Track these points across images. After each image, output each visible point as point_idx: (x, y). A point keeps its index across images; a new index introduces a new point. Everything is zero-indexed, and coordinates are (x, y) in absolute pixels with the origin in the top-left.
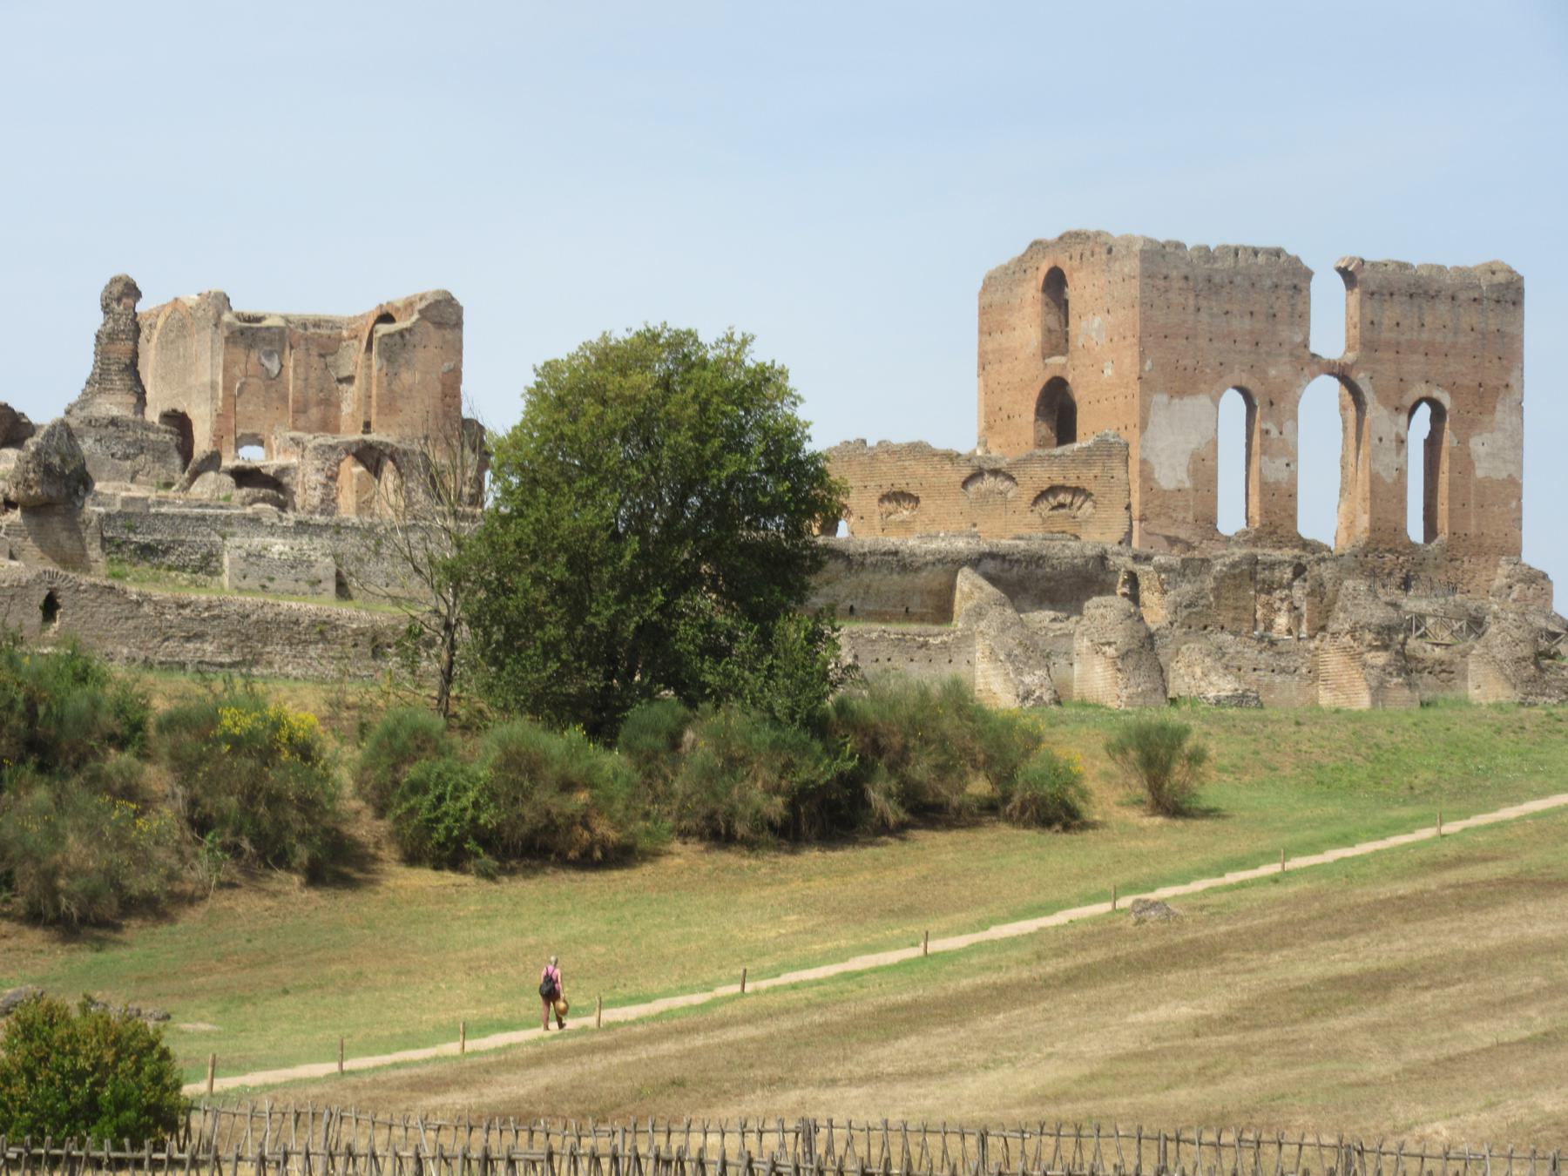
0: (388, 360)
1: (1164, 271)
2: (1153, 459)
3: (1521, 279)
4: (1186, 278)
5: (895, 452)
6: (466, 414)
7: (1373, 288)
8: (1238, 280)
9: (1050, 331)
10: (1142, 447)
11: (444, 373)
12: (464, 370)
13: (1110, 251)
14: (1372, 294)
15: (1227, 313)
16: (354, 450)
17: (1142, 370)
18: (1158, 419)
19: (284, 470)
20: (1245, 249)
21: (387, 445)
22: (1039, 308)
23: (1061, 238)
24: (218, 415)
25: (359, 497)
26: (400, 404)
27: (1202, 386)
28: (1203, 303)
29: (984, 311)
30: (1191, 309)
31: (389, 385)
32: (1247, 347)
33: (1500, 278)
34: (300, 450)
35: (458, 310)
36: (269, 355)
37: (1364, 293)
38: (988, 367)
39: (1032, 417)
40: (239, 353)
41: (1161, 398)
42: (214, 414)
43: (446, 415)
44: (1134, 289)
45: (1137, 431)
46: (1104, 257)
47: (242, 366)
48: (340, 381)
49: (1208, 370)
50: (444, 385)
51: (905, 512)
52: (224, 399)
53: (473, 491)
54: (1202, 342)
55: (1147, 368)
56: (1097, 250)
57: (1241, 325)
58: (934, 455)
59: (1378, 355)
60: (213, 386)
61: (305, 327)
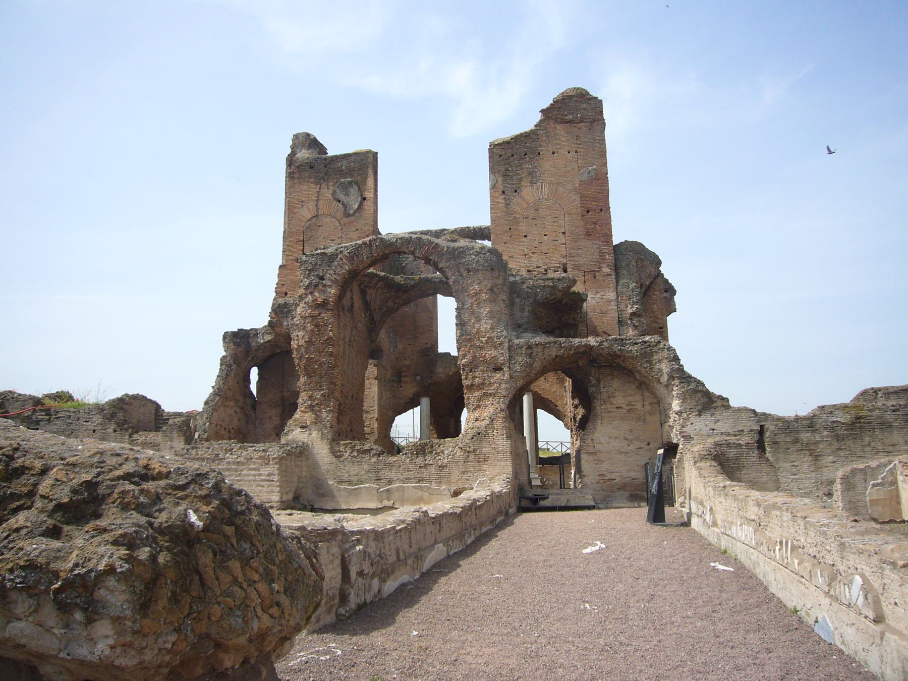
26: (523, 227)
31: (507, 205)
35: (597, 104)
36: (345, 188)
40: (309, 189)
43: (588, 234)
47: (311, 206)
50: (583, 197)
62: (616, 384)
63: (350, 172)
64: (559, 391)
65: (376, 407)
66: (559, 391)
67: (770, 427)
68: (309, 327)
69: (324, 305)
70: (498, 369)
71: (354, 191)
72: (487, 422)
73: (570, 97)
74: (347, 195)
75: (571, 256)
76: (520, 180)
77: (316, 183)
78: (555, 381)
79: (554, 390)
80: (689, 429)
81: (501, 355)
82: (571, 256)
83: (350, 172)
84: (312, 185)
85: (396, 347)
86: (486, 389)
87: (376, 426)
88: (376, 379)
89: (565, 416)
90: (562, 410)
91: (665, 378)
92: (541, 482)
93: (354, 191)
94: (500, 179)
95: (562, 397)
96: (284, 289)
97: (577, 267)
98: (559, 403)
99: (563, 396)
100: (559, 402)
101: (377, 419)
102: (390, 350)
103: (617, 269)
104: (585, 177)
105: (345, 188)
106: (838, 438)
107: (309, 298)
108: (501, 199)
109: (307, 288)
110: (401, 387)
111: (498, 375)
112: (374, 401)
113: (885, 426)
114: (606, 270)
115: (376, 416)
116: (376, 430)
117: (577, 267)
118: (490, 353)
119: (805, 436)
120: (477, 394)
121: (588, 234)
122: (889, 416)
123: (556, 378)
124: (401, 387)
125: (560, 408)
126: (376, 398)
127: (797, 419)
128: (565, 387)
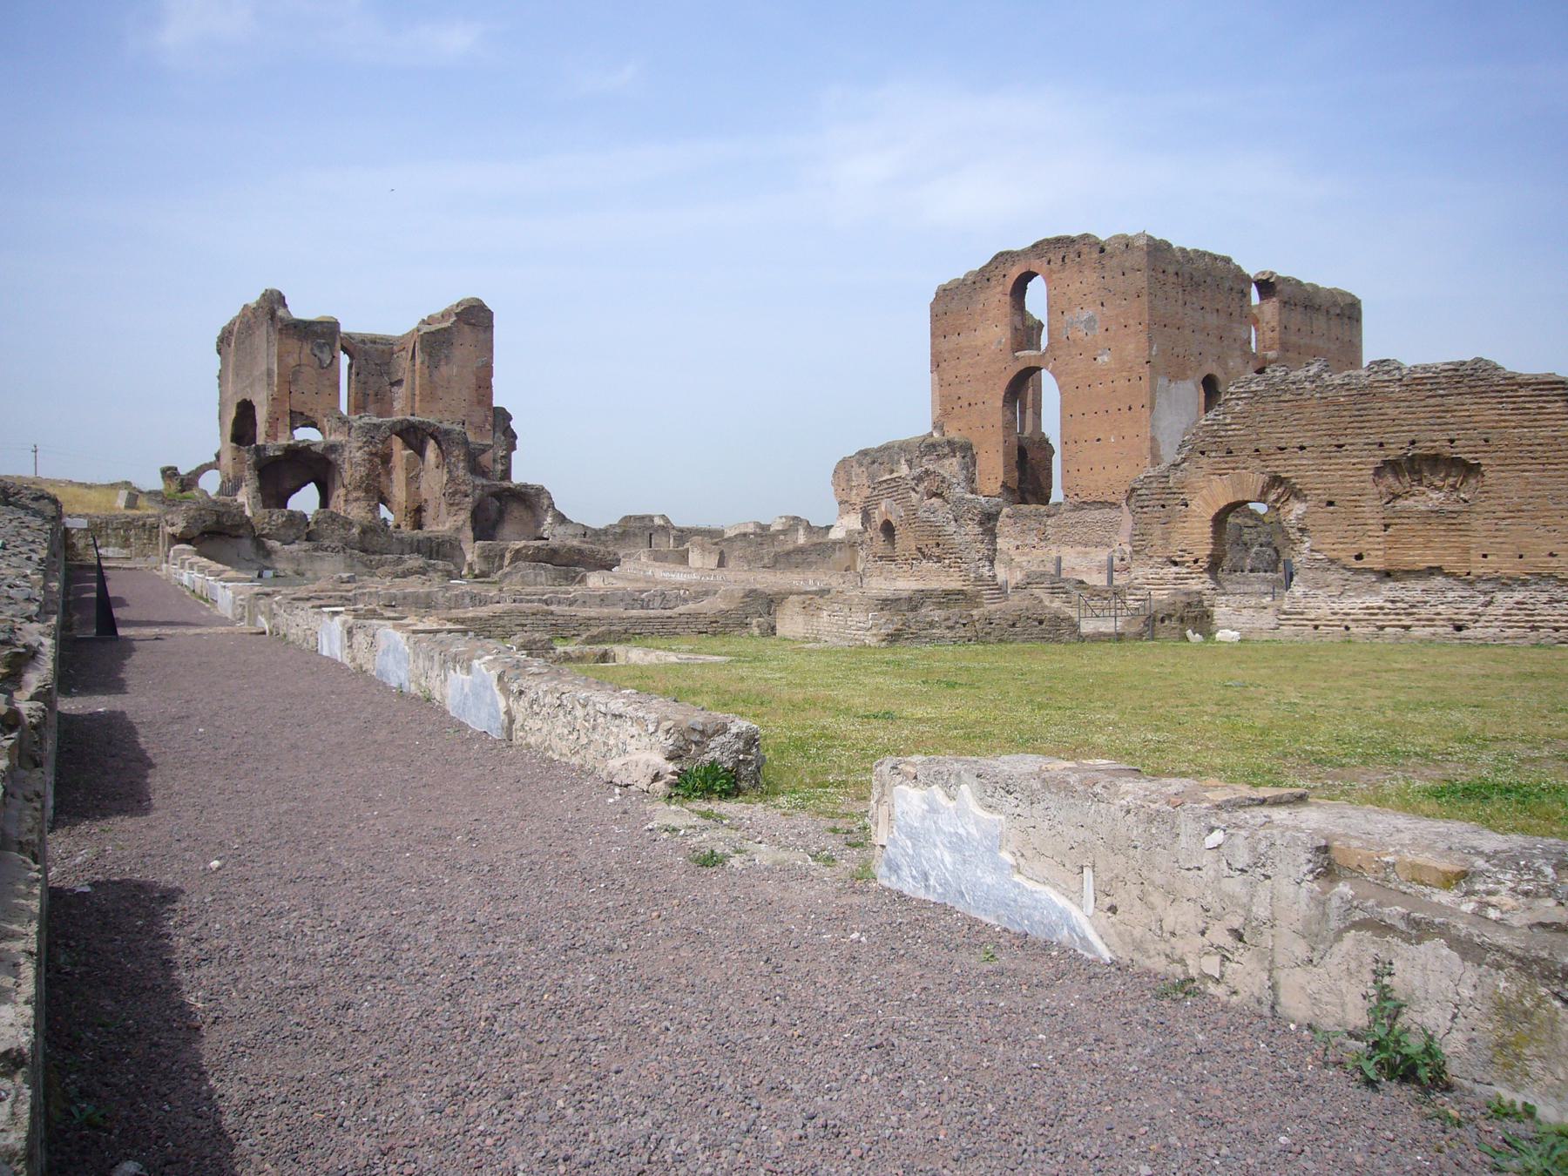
0: (430, 355)
1: (1163, 266)
2: (1160, 439)
3: (1359, 301)
4: (1177, 274)
5: (1420, 381)
6: (495, 404)
7: (1286, 299)
8: (1209, 279)
9: (1016, 329)
10: (1152, 426)
11: (477, 368)
12: (495, 366)
13: (1102, 250)
14: (1285, 303)
15: (1202, 308)
16: (398, 428)
17: (1150, 355)
18: (1161, 401)
19: (332, 448)
20: (1210, 254)
21: (430, 425)
22: (1008, 309)
23: (1035, 246)
24: (273, 399)
25: (408, 473)
27: (1189, 372)
28: (1188, 298)
29: (935, 317)
30: (1180, 302)
32: (1215, 340)
33: (1349, 300)
34: (346, 429)
36: (321, 347)
37: (1285, 303)
38: (943, 365)
39: (1000, 403)
40: (292, 344)
41: (1162, 381)
42: (270, 398)
44: (1140, 280)
45: (1146, 411)
46: (1095, 255)
47: (296, 356)
48: (392, 384)
49: (1192, 359)
51: (1434, 495)
52: (279, 385)
53: (503, 468)
54: (1187, 332)
55: (1154, 353)
56: (1085, 250)
57: (1213, 320)
58: (1521, 386)
59: (1289, 355)
60: (269, 373)
61: (363, 342)
62: (515, 505)
63: (322, 335)
67: (589, 533)
68: (368, 466)
69: (376, 454)
70: (467, 496)
71: (327, 349)
72: (461, 522)
73: (474, 306)
74: (322, 352)
75: (469, 416)
76: (440, 360)
77: (299, 340)
80: (555, 532)
81: (469, 489)
82: (469, 416)
83: (322, 335)
84: (296, 341)
86: (461, 506)
91: (545, 507)
93: (327, 349)
94: (427, 358)
96: (276, 416)
97: (471, 423)
103: (494, 427)
104: (480, 364)
105: (321, 347)
106: (616, 539)
107: (366, 449)
108: (427, 371)
109: (365, 442)
111: (467, 499)
113: (635, 535)
114: (488, 427)
117: (471, 423)
118: (463, 488)
119: (603, 538)
120: (456, 508)
121: (479, 403)
122: (637, 531)
127: (600, 530)
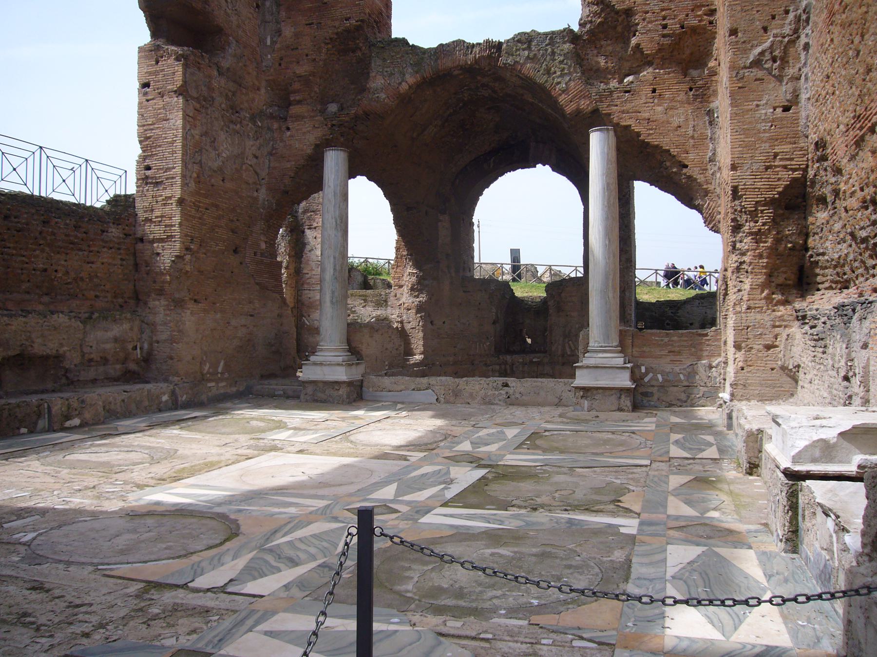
64: (691, 123)
65: (178, 170)
66: (691, 123)
78: (682, 96)
79: (676, 121)
85: (279, 32)
87: (177, 219)
88: (179, 92)
89: (707, 193)
90: (700, 178)
92: (633, 379)
95: (701, 141)
98: (690, 158)
99: (703, 137)
100: (691, 156)
101: (181, 202)
102: (262, 41)
110: (288, 129)
112: (174, 152)
115: (177, 192)
116: (177, 234)
123: (685, 87)
124: (288, 129)
125: (693, 171)
126: (179, 144)
128: (710, 113)
